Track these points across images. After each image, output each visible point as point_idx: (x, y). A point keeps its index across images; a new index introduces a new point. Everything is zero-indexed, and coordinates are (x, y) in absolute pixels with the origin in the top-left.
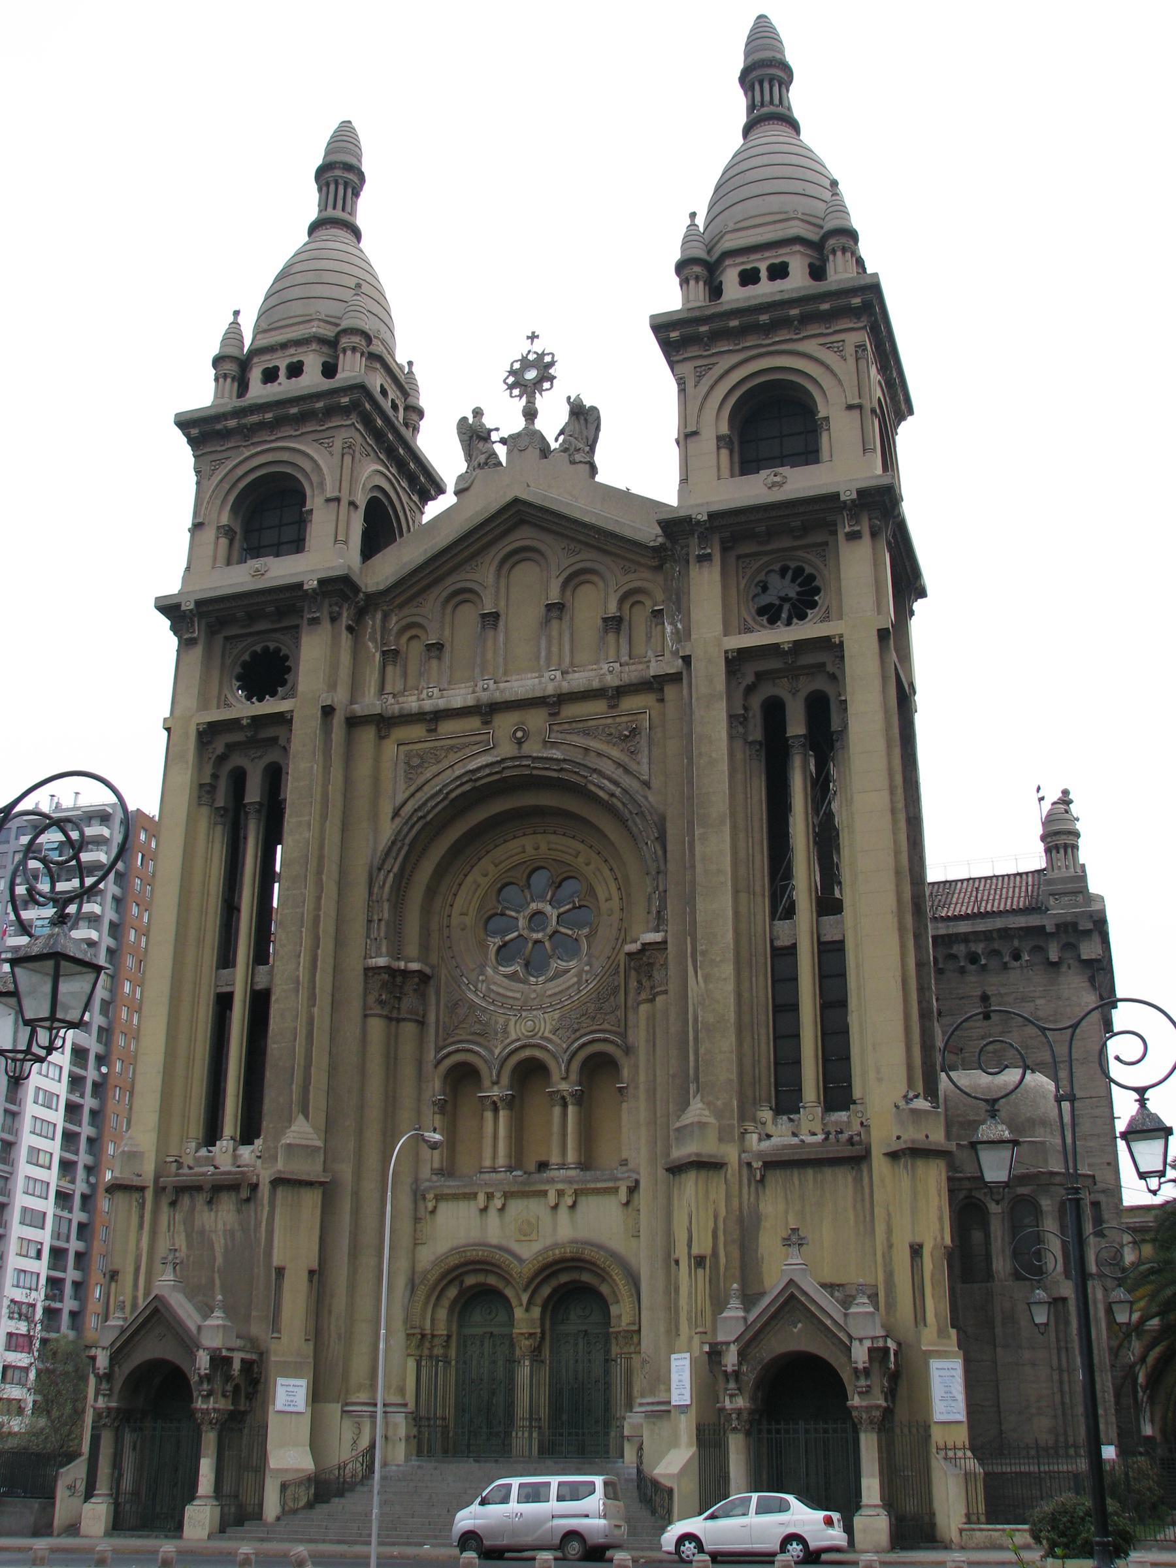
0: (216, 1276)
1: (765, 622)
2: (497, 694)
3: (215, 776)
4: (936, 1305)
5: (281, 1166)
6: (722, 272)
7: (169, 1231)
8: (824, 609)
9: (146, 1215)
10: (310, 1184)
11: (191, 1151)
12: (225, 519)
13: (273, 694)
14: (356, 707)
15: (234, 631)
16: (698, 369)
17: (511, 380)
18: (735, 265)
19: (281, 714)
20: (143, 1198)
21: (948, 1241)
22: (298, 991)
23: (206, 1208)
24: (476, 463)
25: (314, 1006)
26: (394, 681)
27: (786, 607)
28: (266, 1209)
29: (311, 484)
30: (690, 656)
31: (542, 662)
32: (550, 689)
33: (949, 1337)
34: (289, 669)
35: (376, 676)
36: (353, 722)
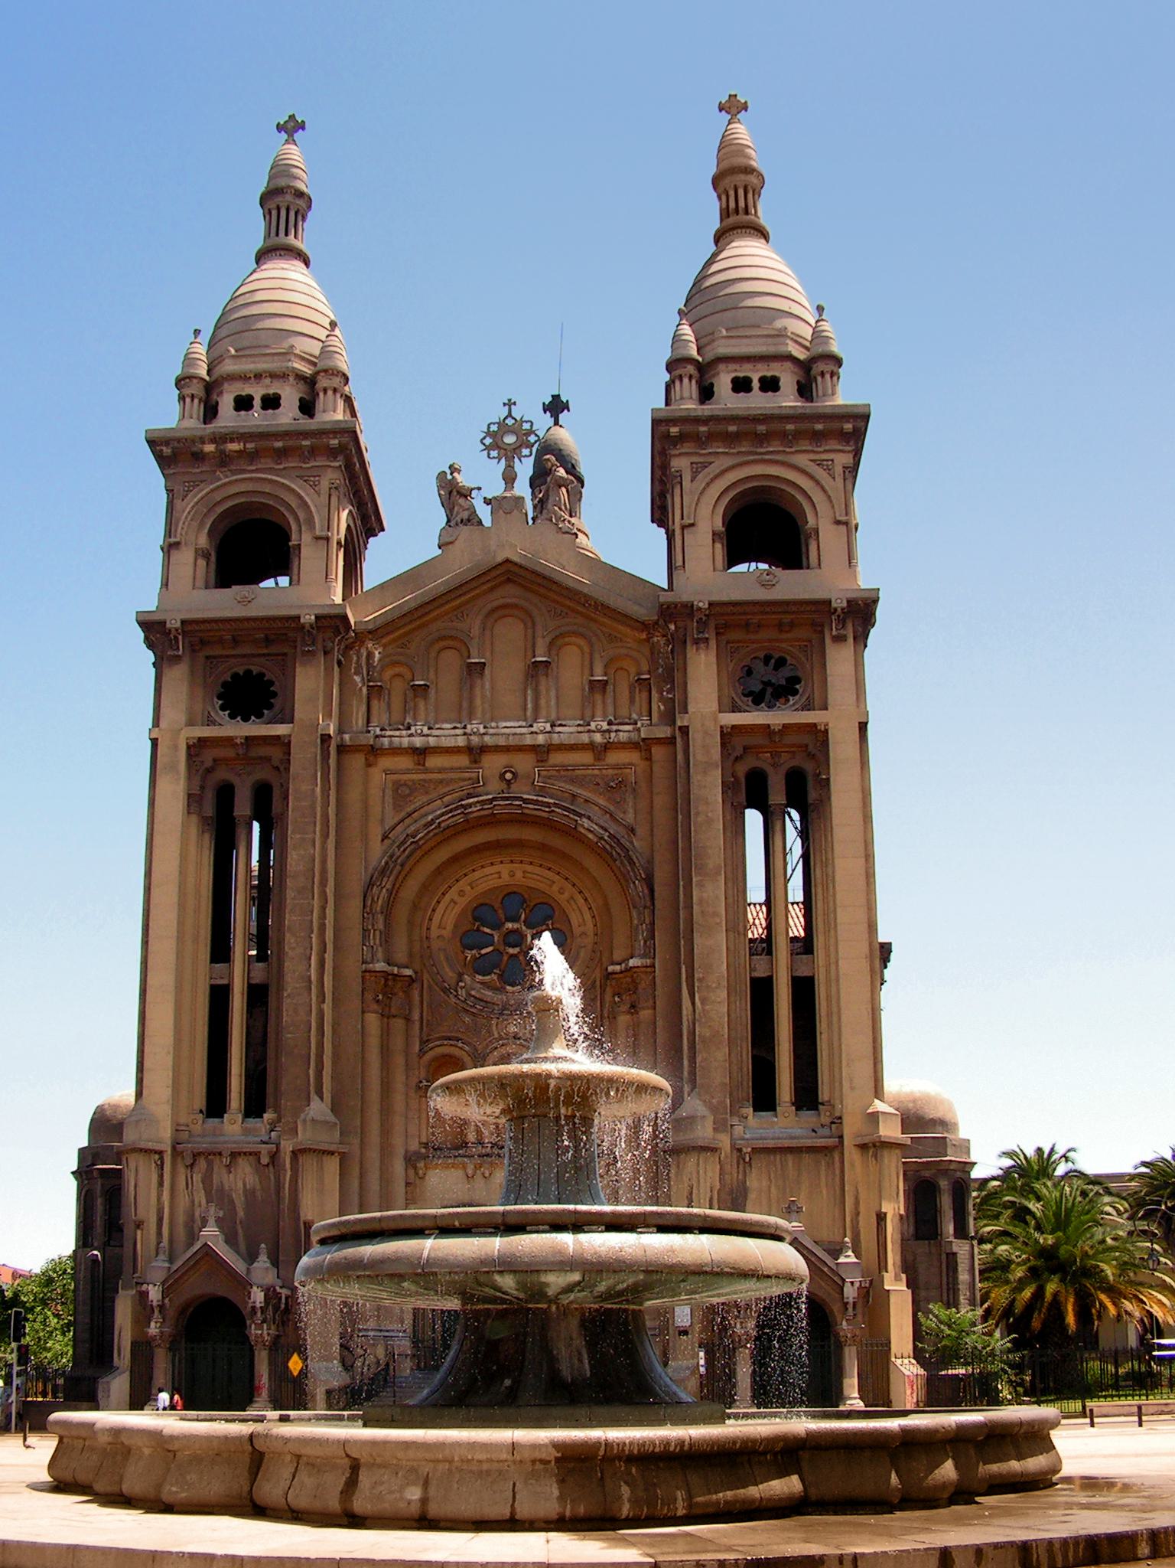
0: (239, 1227)
1: (750, 703)
2: (487, 738)
3: (202, 788)
4: (893, 1257)
5: (305, 1136)
6: (714, 376)
7: (187, 1188)
8: (805, 698)
9: (165, 1174)
10: (332, 1153)
11: (200, 1125)
12: (203, 541)
13: (259, 715)
14: (347, 737)
15: (218, 651)
16: (694, 466)
17: (488, 441)
18: (728, 372)
19: (278, 737)
20: (162, 1159)
21: (902, 1212)
22: (311, 989)
23: (224, 1171)
24: (458, 519)
25: (323, 1002)
26: (380, 715)
27: (769, 690)
28: (289, 1173)
29: (297, 519)
30: (688, 727)
31: (529, 713)
32: (541, 739)
33: (901, 1280)
34: (274, 695)
35: (364, 708)
36: (342, 749)
